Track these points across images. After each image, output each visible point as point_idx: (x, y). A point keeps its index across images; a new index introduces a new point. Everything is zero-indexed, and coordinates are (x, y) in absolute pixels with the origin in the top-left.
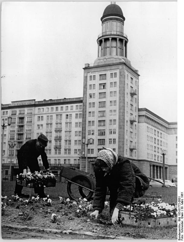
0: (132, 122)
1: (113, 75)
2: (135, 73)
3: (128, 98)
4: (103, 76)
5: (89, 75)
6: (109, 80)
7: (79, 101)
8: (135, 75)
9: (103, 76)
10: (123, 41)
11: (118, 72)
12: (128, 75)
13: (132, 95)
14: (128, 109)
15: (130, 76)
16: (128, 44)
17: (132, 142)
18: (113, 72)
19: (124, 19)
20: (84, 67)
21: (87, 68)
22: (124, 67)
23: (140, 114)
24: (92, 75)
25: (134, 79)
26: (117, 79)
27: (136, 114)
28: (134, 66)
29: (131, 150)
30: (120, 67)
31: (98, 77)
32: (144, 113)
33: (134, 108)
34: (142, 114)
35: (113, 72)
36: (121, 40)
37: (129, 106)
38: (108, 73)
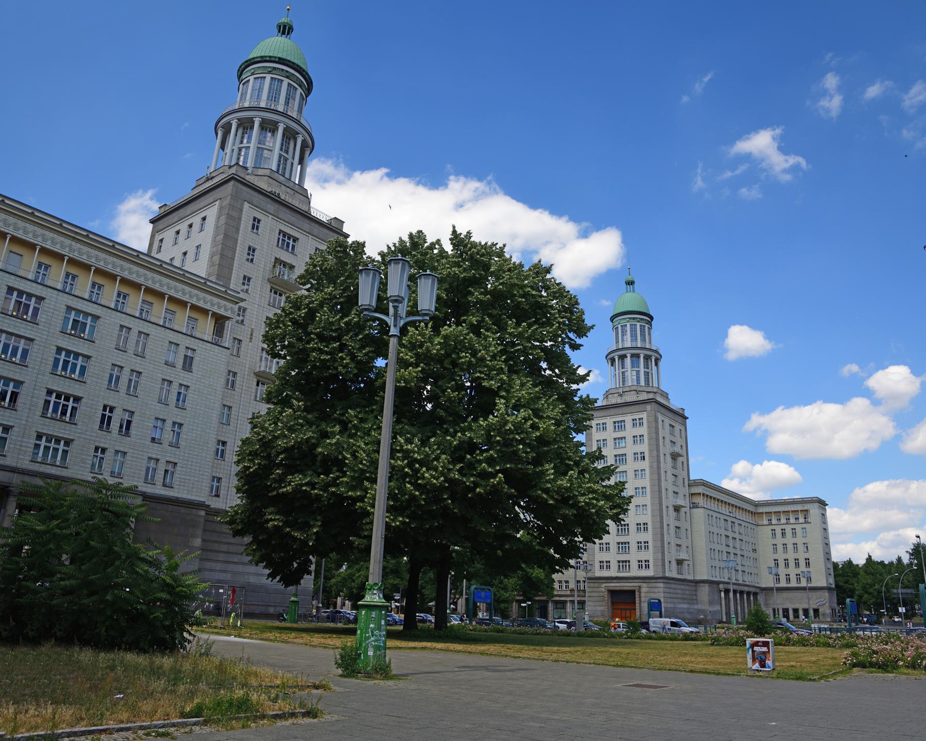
0: (677, 509)
1: (636, 423)
2: (681, 416)
3: (667, 464)
4: (619, 426)
6: (630, 431)
8: (680, 419)
9: (619, 426)
10: (653, 358)
11: (644, 415)
12: (665, 421)
13: (675, 456)
14: (667, 483)
15: (667, 421)
16: (661, 364)
17: (680, 546)
18: (637, 416)
19: (652, 318)
23: (693, 492)
24: (601, 422)
25: (678, 427)
26: (643, 430)
28: (675, 404)
29: (680, 562)
30: (648, 407)
31: (610, 426)
32: (700, 490)
34: (697, 491)
35: (637, 416)
36: (647, 358)
37: (671, 479)
38: (628, 419)
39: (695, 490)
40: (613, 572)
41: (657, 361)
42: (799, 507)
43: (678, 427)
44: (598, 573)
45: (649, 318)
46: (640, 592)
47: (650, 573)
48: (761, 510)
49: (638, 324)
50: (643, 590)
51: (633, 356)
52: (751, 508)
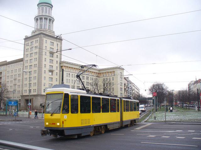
2: (59, 39)
5: (26, 43)
7: (21, 60)
8: (60, 41)
10: (51, 20)
11: (38, 39)
13: (52, 53)
15: (49, 41)
16: (54, 22)
18: (36, 39)
20: (24, 38)
21: (27, 39)
22: (42, 36)
27: (56, 66)
28: (57, 34)
33: (55, 62)
37: (48, 60)
38: (34, 40)
39: (62, 65)
40: (27, 94)
41: (53, 21)
42: (111, 71)
43: (55, 43)
44: (24, 94)
45: (51, 6)
46: (33, 100)
47: (36, 93)
48: (101, 72)
49: (44, 7)
50: (34, 99)
51: (45, 18)
52: (97, 72)
